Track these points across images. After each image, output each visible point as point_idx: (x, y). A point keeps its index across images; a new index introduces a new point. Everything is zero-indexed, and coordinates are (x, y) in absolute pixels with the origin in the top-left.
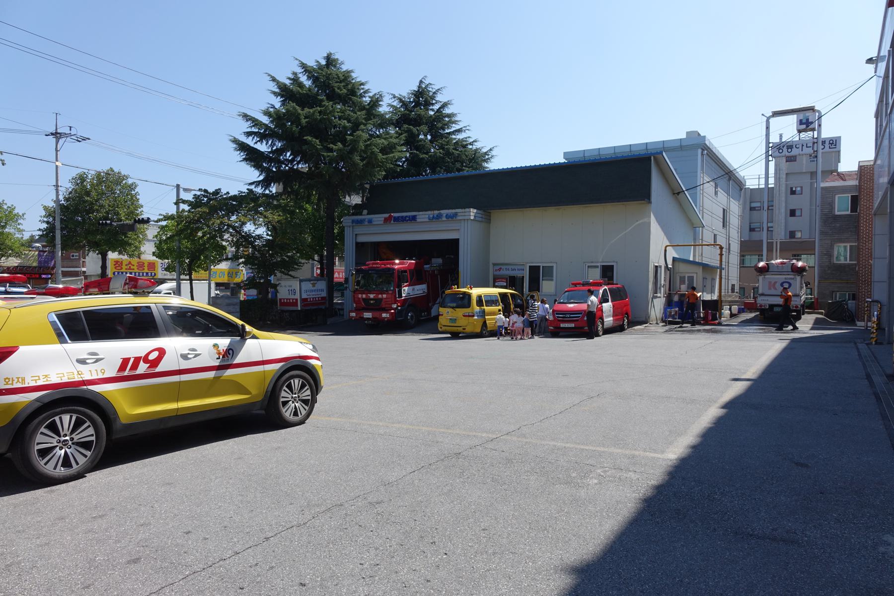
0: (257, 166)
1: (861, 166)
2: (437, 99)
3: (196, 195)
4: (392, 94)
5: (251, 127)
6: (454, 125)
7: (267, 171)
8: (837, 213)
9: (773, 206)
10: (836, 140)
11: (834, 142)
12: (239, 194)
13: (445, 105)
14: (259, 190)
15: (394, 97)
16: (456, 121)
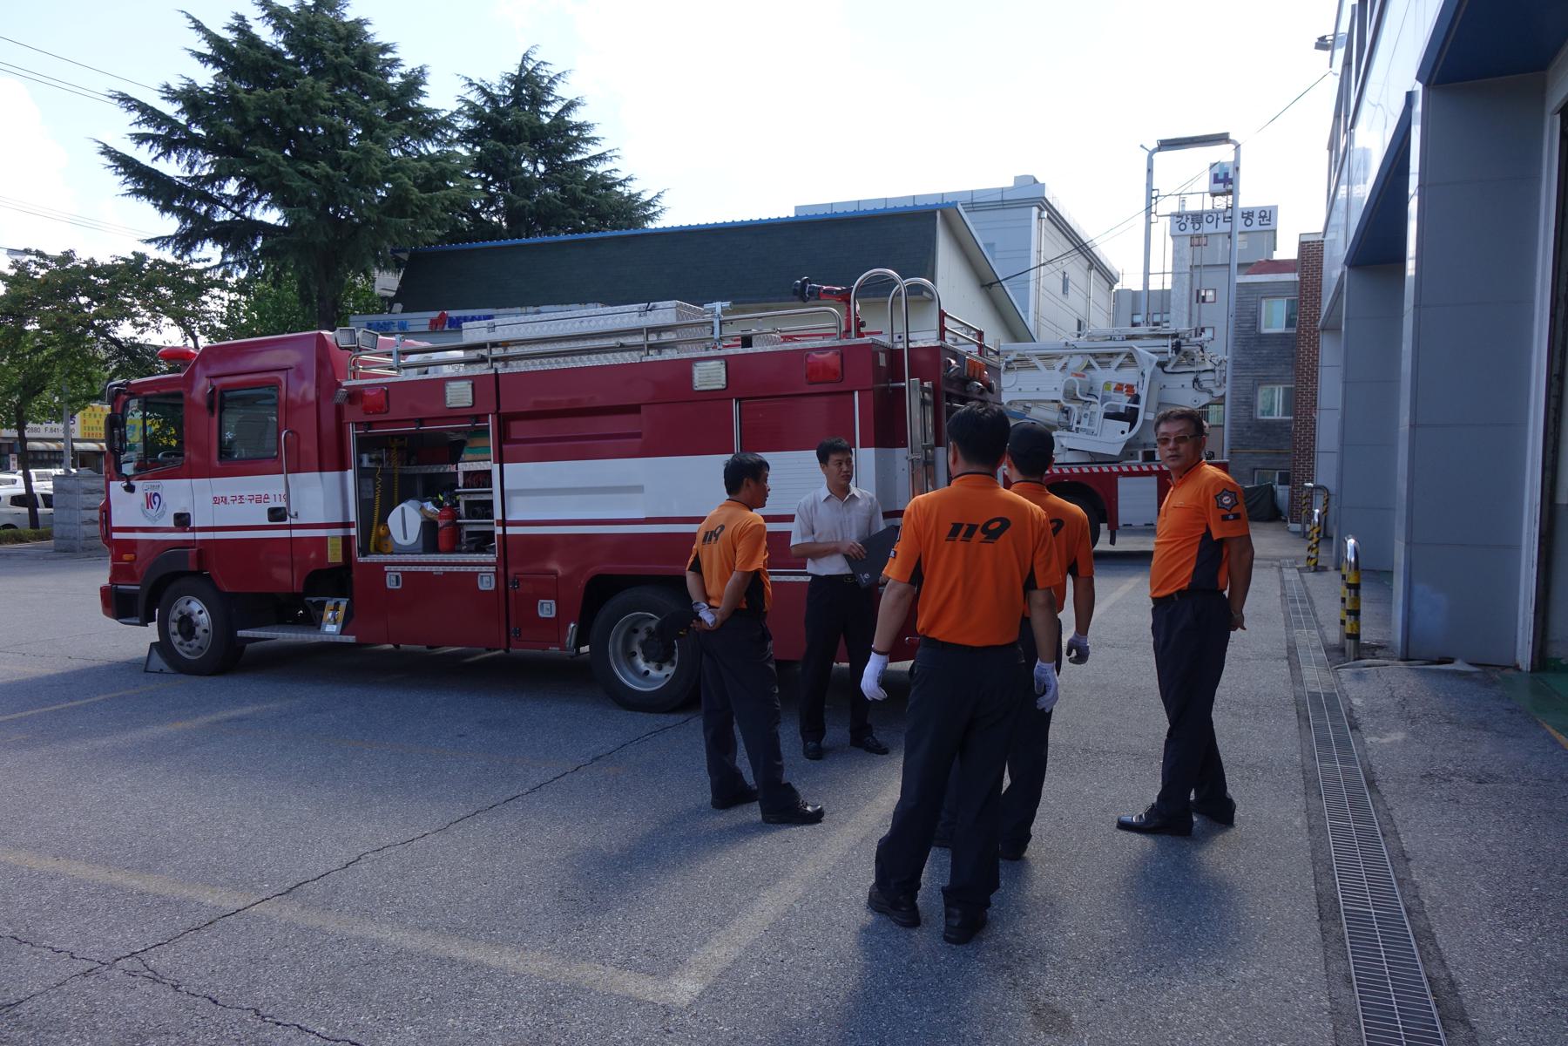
0: (166, 208)
1: (1303, 242)
2: (557, 92)
3: (17, 261)
4: (466, 78)
5: (139, 123)
6: (590, 146)
7: (185, 214)
8: (1265, 331)
9: (1168, 322)
10: (1270, 212)
11: (1268, 215)
12: (113, 262)
13: (570, 106)
14: (168, 255)
15: (471, 84)
16: (595, 138)
